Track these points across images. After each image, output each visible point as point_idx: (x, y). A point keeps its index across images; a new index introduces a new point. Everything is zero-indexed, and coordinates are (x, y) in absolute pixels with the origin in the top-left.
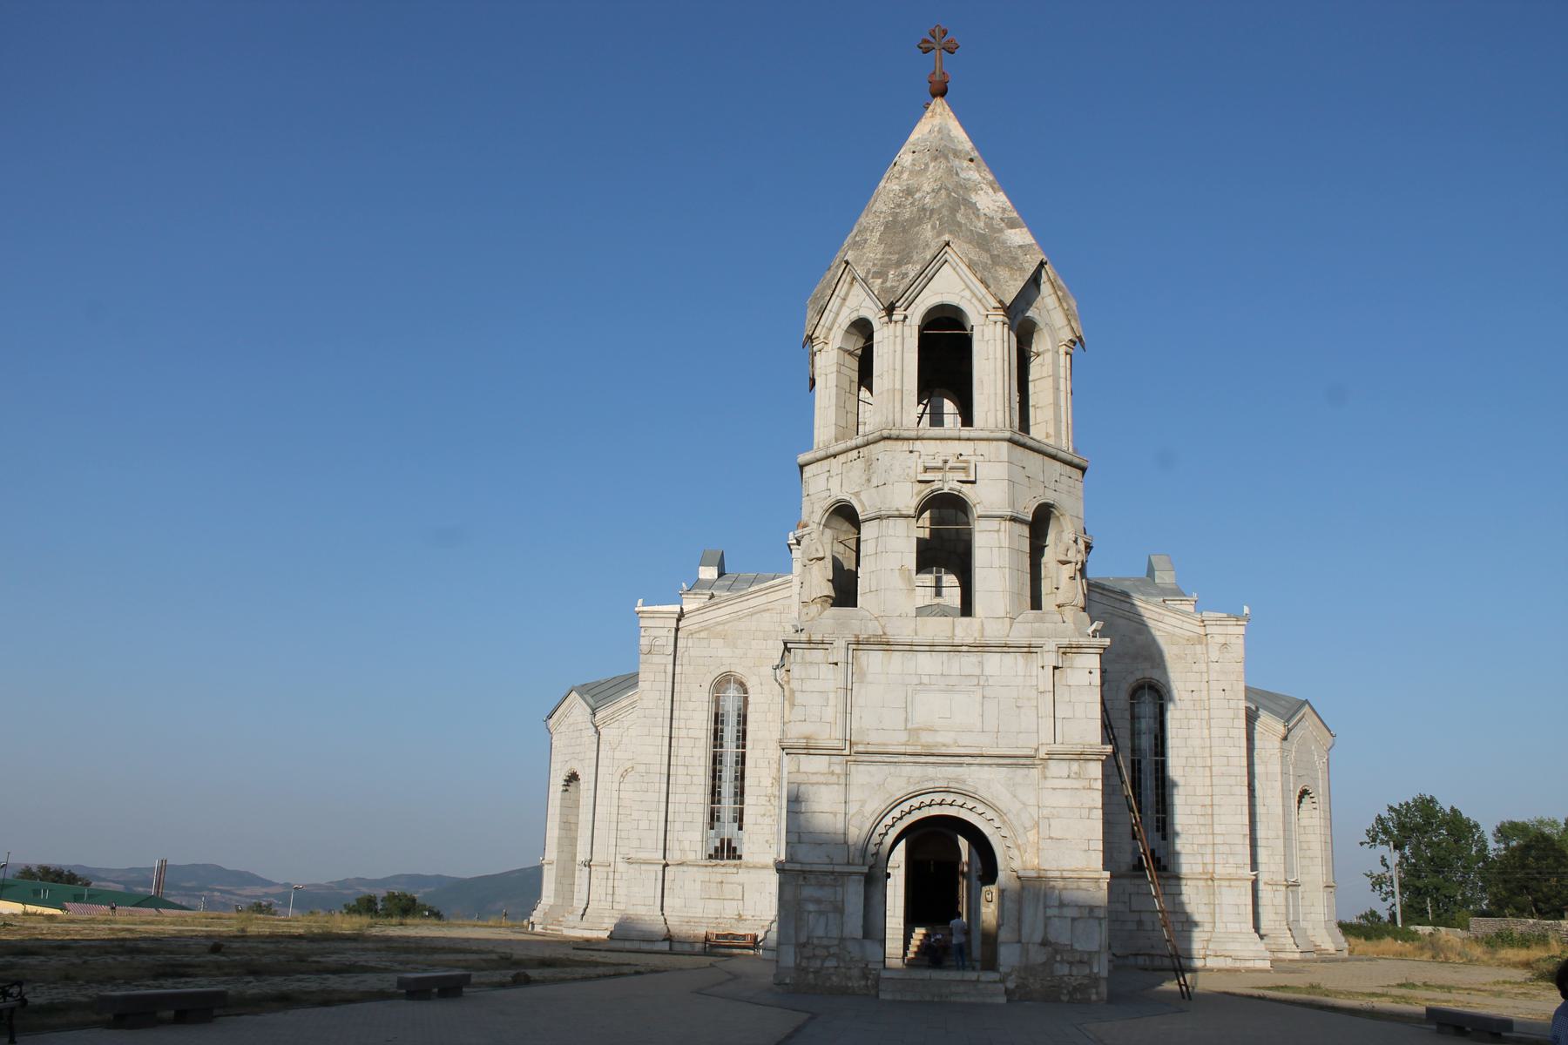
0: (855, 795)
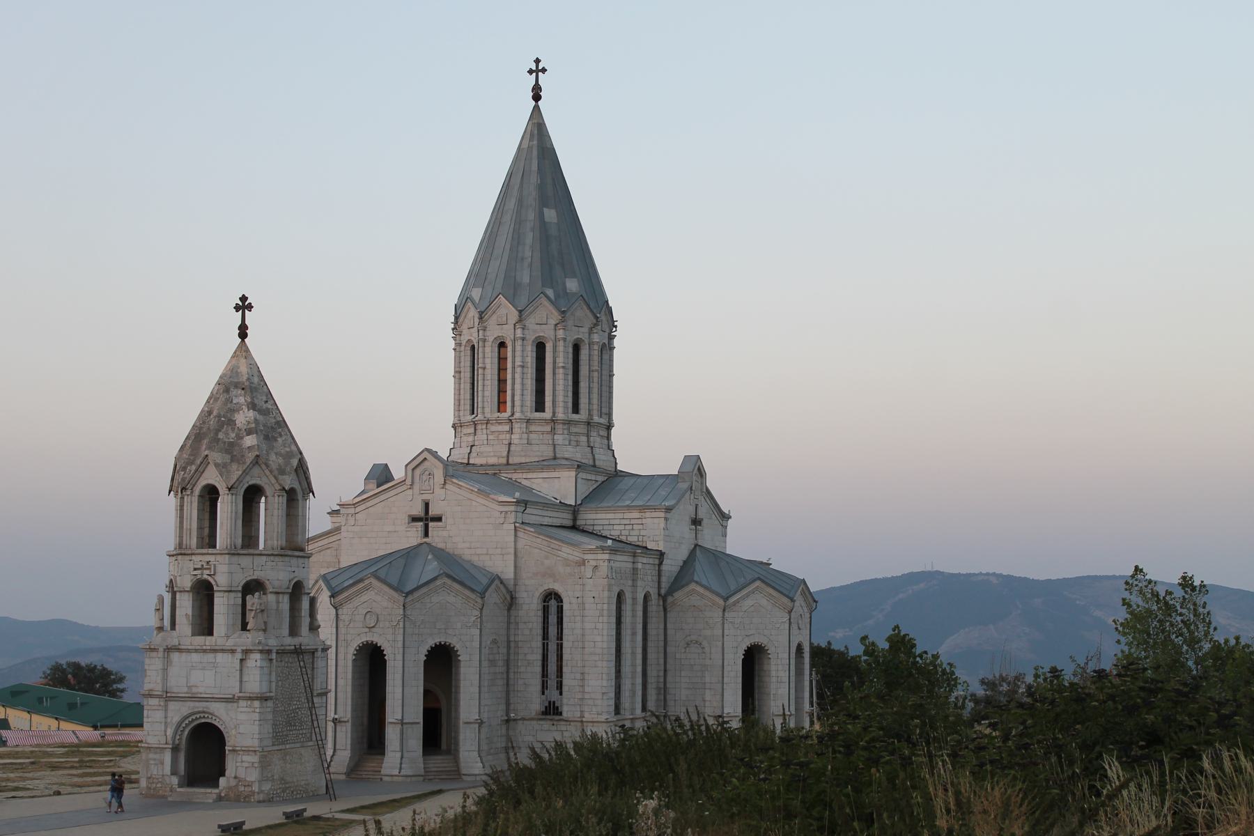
0: (170, 714)
